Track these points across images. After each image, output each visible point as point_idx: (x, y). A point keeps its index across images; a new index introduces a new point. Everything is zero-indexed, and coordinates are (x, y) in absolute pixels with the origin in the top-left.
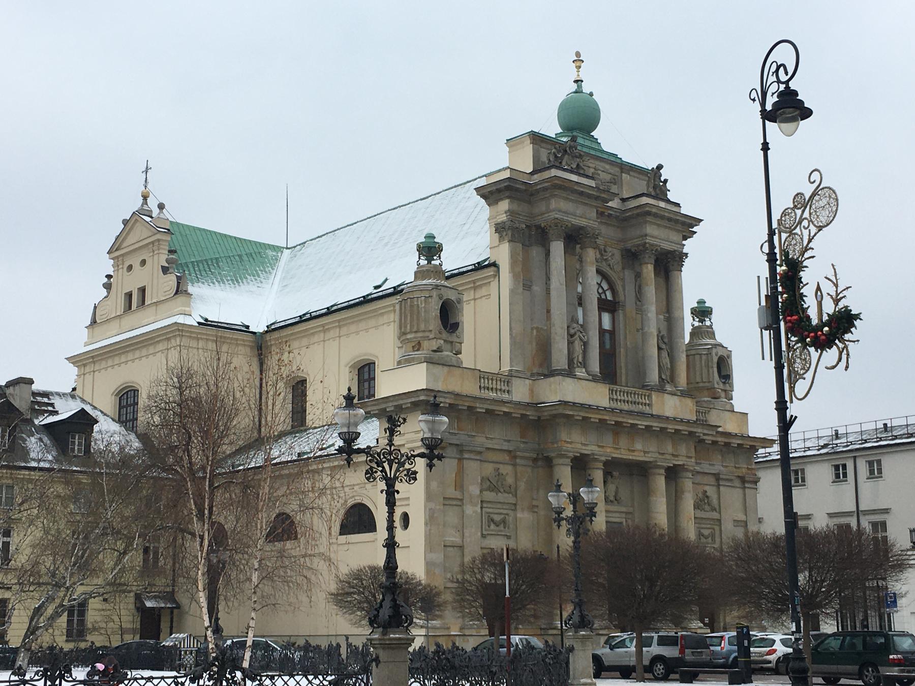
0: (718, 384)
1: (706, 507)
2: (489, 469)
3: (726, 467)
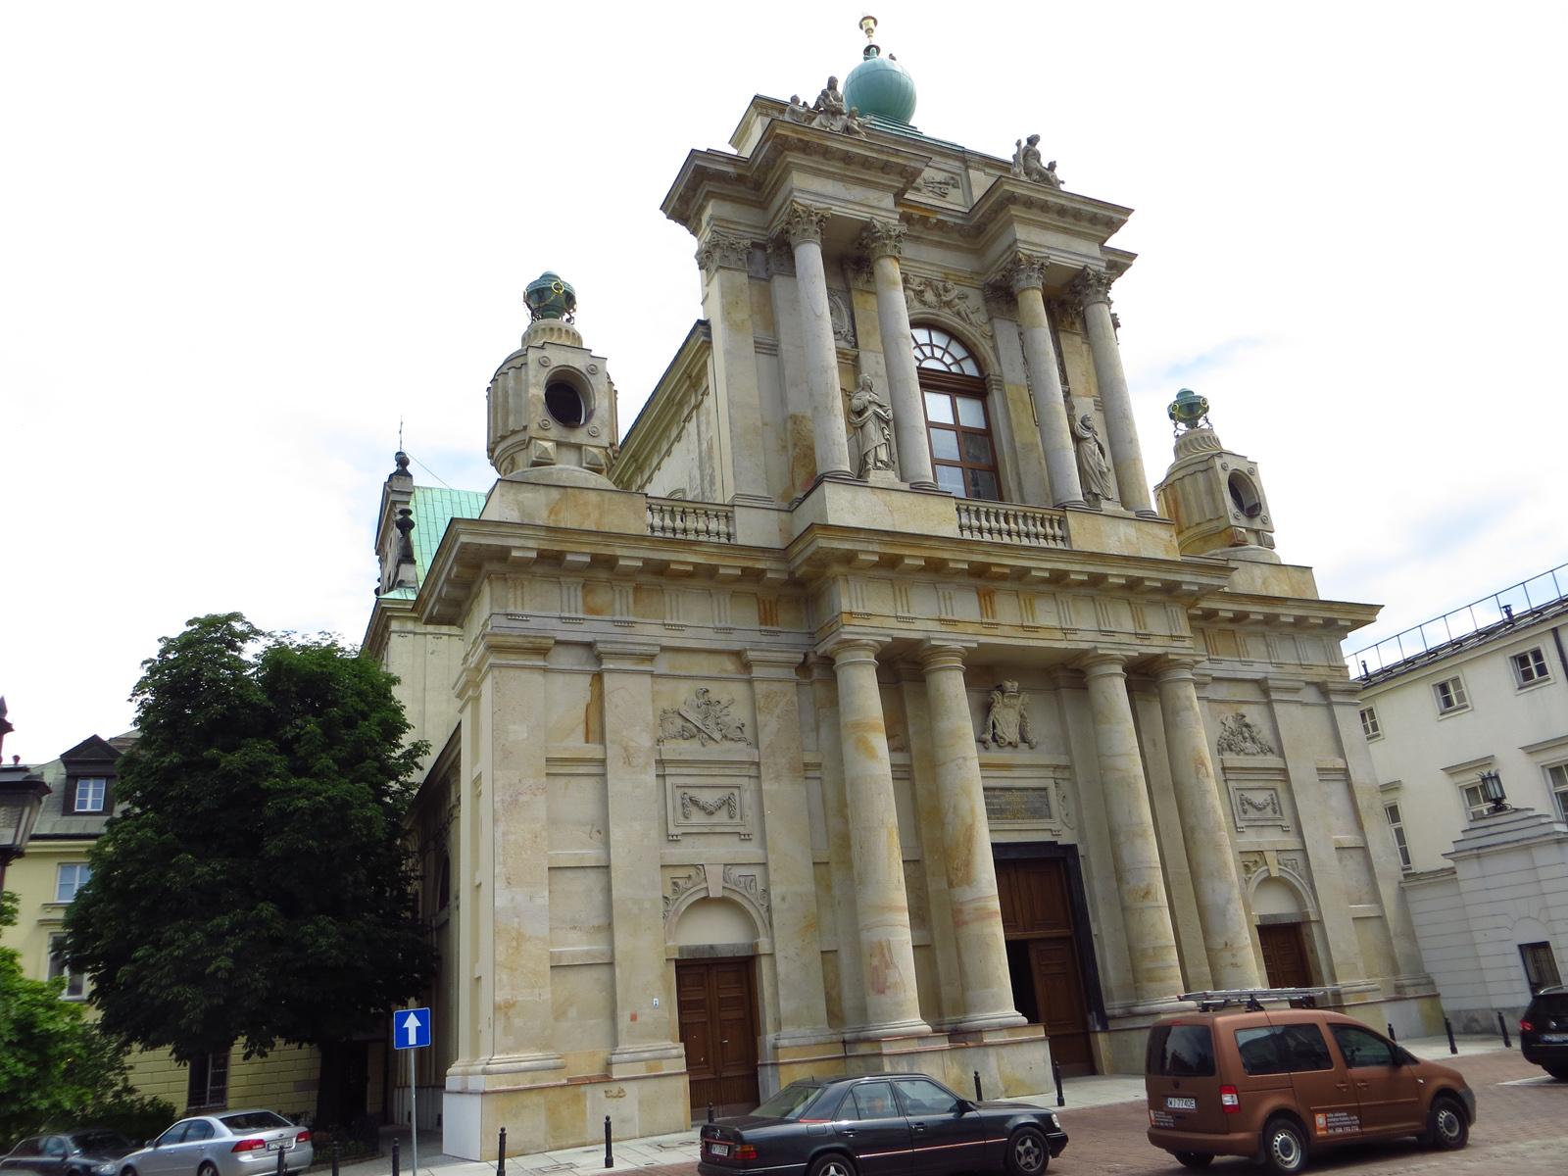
0: (1236, 518)
1: (1254, 748)
2: (683, 694)
3: (1279, 665)
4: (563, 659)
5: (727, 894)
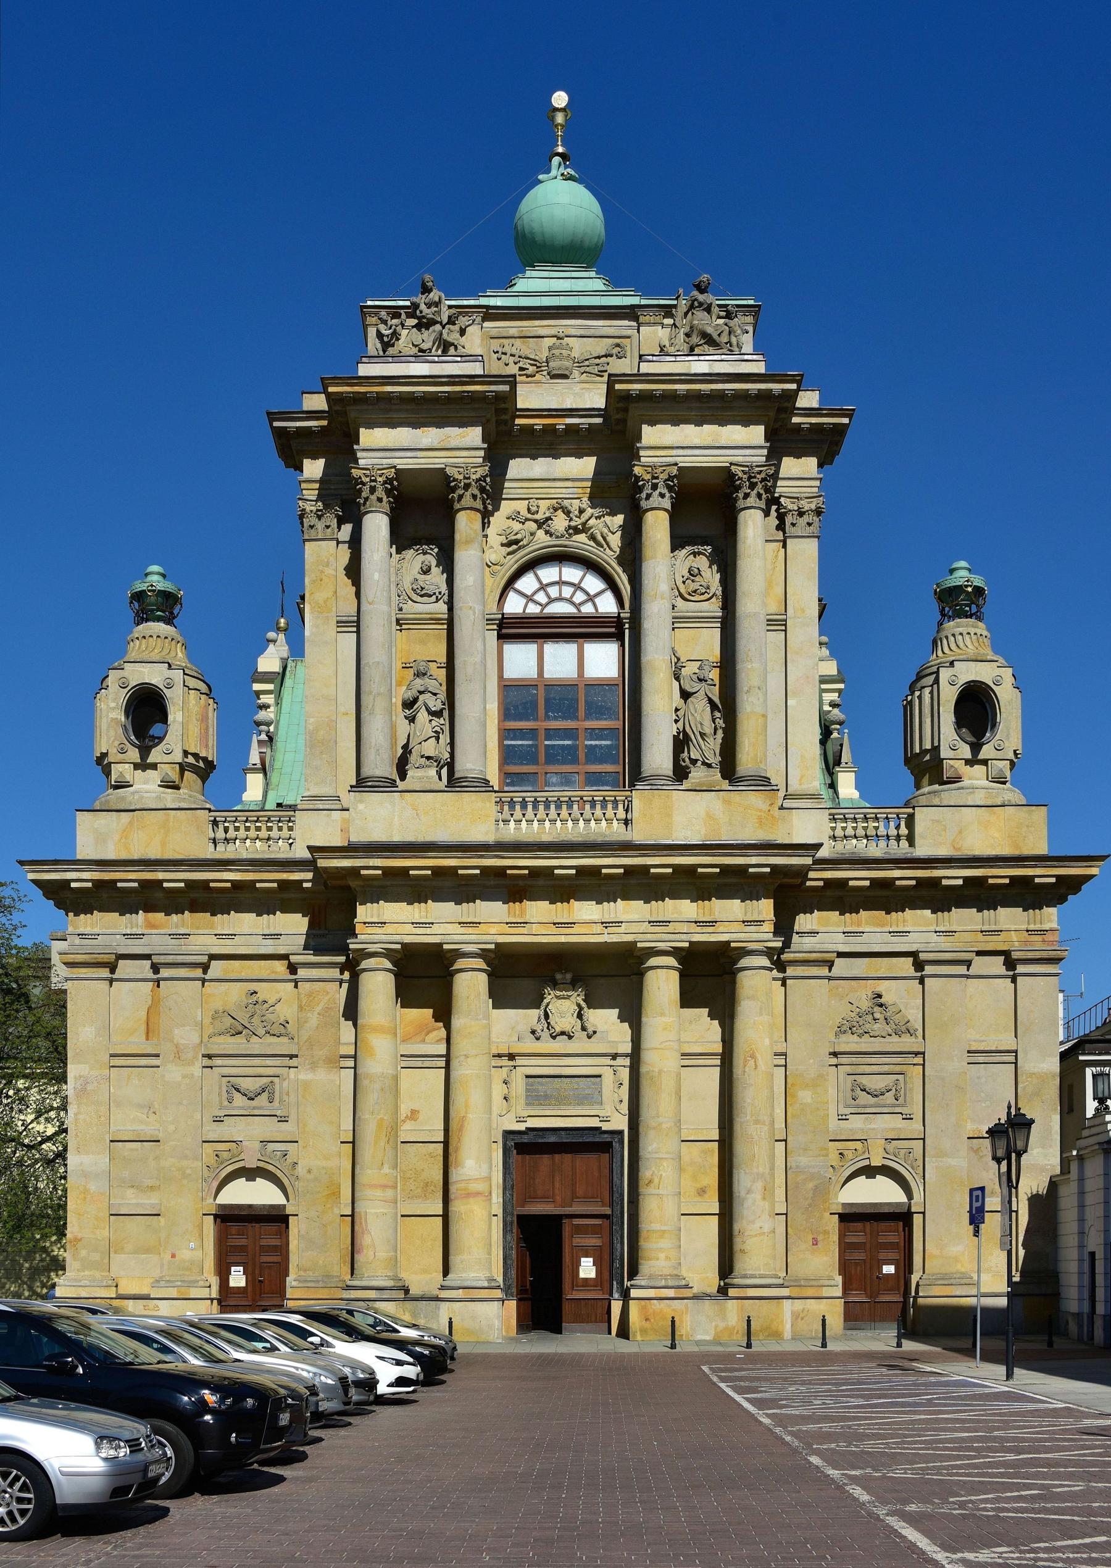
1: (879, 1027)
4: (125, 968)
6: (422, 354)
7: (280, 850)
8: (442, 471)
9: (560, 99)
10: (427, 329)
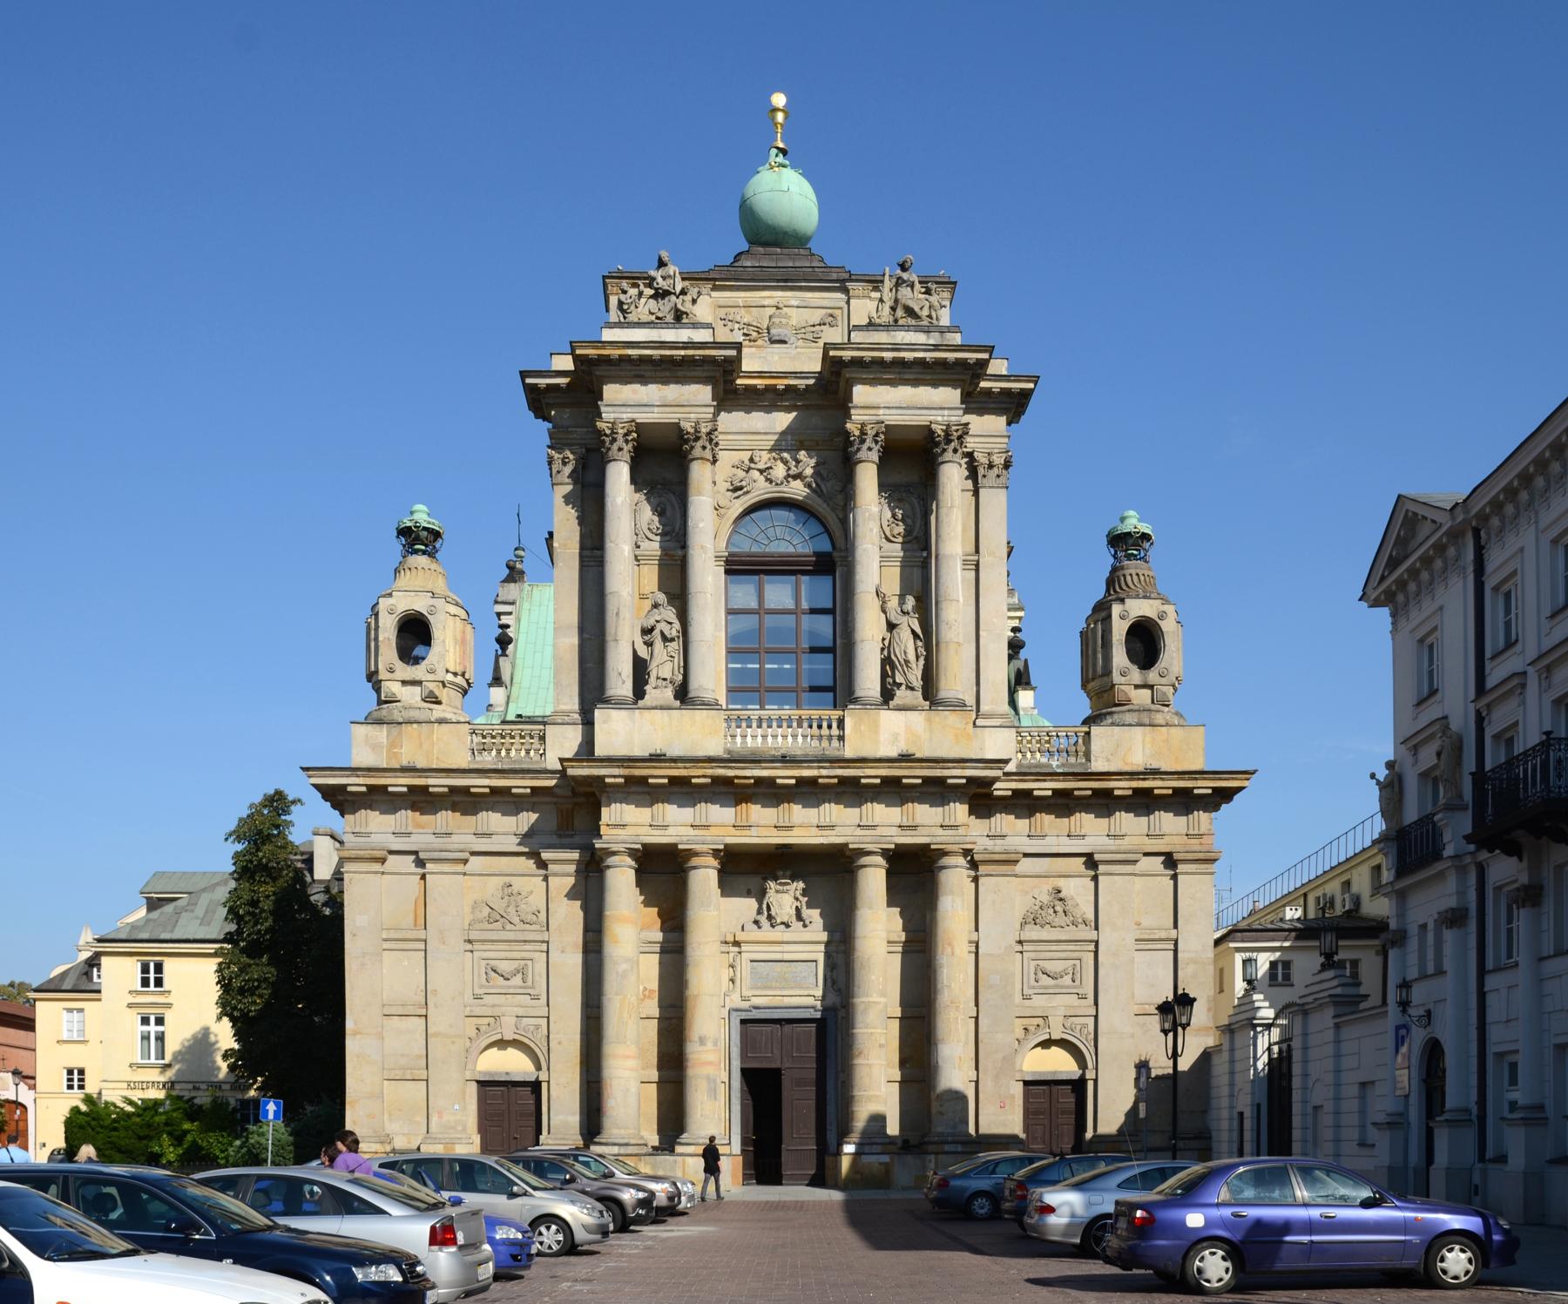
1: (1060, 919)
5: (517, 1037)
6: (658, 322)
7: (534, 760)
8: (677, 425)
9: (779, 100)
10: (663, 299)
